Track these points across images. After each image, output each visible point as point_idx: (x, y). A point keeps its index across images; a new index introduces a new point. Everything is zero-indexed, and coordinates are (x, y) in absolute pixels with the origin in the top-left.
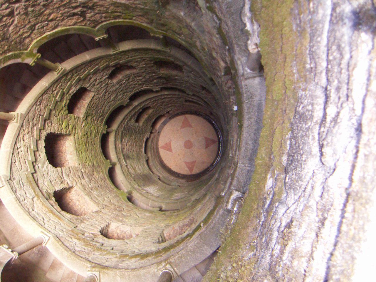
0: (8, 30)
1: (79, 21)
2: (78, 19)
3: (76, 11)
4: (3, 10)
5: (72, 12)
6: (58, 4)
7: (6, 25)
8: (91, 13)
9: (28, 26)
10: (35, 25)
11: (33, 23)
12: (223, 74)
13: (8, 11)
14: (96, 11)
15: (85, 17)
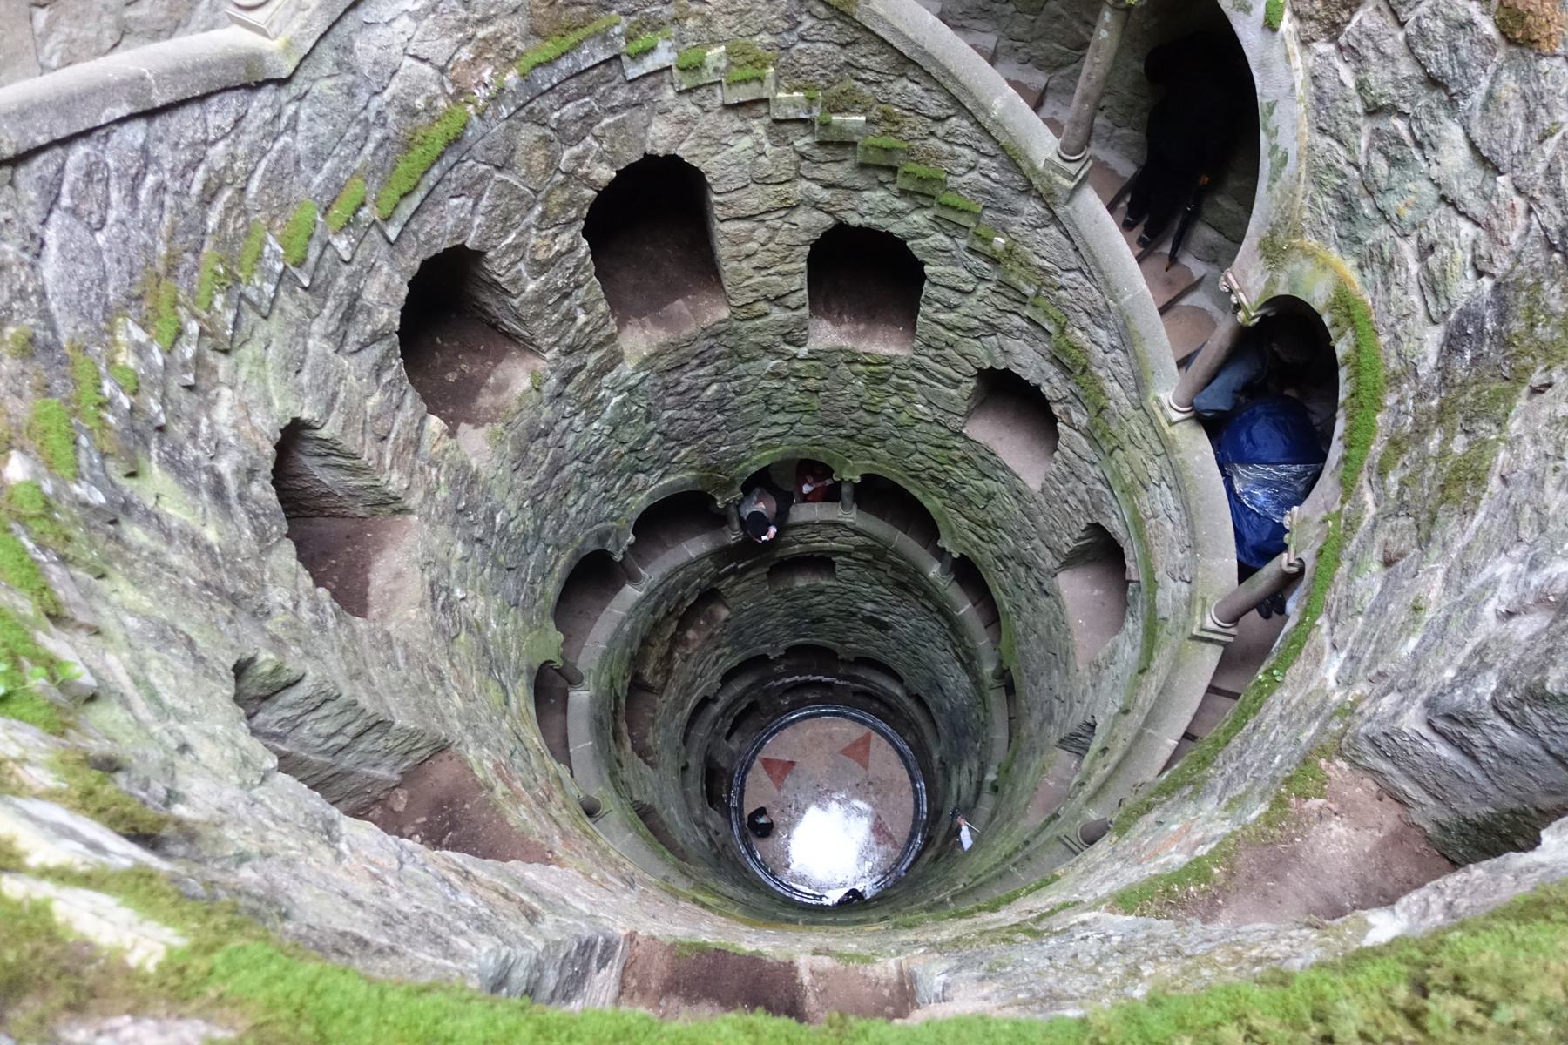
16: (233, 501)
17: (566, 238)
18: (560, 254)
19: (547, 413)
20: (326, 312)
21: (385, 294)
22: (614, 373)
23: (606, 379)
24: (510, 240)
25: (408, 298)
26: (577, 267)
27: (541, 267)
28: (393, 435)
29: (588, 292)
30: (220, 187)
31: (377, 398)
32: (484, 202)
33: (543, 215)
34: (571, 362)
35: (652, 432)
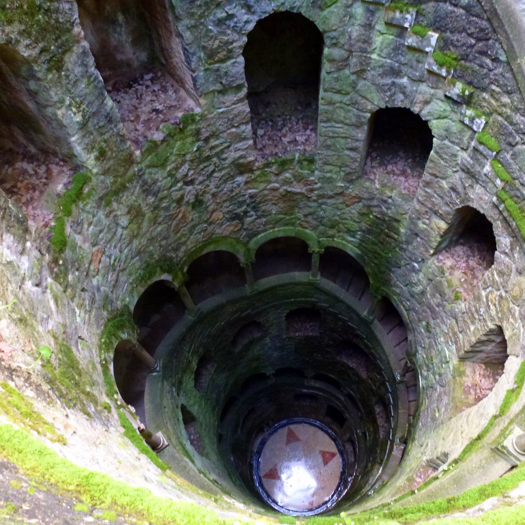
0: (171, 224)
1: (237, 229)
2: (236, 226)
3: (238, 211)
4: (177, 190)
5: (235, 212)
6: (226, 195)
7: (172, 215)
8: (252, 216)
9: (189, 226)
10: (194, 227)
11: (194, 222)
12: (432, 252)
13: (181, 192)
14: (259, 213)
15: (243, 224)
16: (393, 79)
17: (493, 313)
18: (489, 307)
19: (448, 307)
20: (469, 159)
21: (481, 199)
22: (455, 351)
23: (454, 347)
24: (496, 276)
25: (478, 212)
26: (484, 319)
27: (487, 297)
28: (435, 195)
29: (478, 329)
30: (497, 100)
31: (446, 186)
32: (507, 259)
33: (501, 297)
34: (461, 324)
35: (435, 379)
